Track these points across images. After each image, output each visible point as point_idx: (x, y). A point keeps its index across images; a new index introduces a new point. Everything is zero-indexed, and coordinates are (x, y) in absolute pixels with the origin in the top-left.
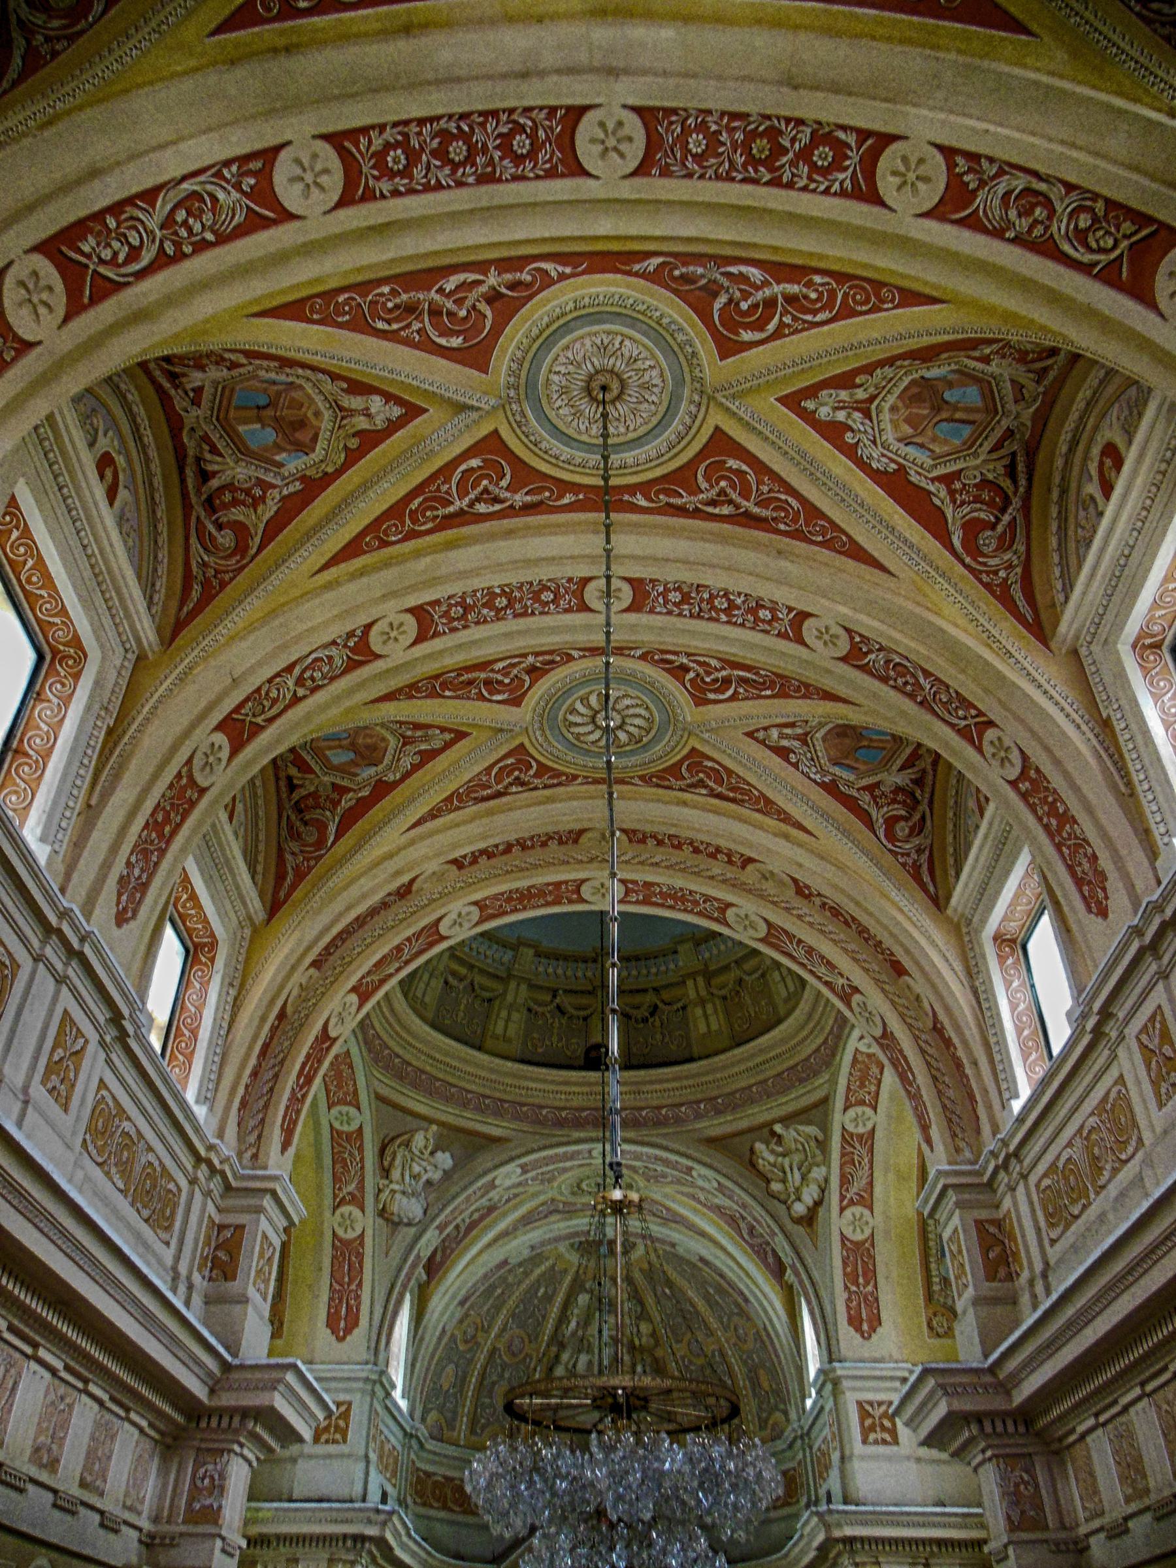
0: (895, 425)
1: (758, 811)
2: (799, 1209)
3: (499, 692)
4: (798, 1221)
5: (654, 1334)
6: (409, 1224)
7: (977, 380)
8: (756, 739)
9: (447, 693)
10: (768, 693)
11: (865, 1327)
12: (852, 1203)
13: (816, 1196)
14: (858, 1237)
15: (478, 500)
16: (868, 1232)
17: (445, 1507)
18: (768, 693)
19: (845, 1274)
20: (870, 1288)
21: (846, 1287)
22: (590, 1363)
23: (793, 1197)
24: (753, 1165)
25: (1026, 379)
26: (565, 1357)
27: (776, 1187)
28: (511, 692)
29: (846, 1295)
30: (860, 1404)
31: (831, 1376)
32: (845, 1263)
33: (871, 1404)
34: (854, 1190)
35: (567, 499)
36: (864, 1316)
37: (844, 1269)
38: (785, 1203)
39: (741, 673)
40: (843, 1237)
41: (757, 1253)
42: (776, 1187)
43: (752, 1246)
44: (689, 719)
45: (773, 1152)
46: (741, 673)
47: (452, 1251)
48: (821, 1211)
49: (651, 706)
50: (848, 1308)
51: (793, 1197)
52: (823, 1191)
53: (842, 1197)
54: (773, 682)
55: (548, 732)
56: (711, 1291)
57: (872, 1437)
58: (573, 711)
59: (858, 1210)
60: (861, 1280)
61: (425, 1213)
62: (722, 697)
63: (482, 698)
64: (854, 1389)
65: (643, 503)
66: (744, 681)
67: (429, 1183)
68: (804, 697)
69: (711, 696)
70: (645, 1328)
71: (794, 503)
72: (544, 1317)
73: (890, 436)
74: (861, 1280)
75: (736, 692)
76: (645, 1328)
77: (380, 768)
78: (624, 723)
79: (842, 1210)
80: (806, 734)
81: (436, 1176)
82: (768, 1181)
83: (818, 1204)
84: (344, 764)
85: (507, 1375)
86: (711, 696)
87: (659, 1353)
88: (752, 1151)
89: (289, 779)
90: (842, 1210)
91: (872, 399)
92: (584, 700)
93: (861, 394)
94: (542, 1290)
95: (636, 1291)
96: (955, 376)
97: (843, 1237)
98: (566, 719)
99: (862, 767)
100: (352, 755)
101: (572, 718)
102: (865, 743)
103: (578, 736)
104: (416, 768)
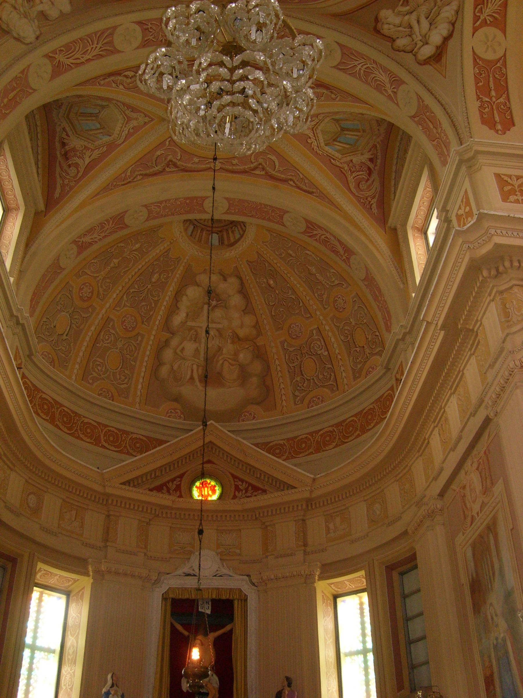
2: (427, 51)
4: (426, 62)
5: (257, 326)
6: (18, 39)
11: (499, 127)
12: (485, 23)
13: (445, 33)
14: (490, 56)
16: (500, 53)
17: (52, 421)
19: (477, 88)
20: (501, 100)
21: (478, 98)
22: (197, 350)
23: (420, 44)
24: (377, 31)
26: (174, 342)
27: (401, 42)
29: (478, 104)
30: (498, 176)
31: (466, 157)
32: (477, 80)
33: (510, 177)
34: (487, 11)
36: (497, 119)
37: (477, 84)
38: (411, 52)
40: (476, 57)
41: (363, 205)
42: (401, 42)
43: (358, 199)
45: (399, 14)
47: (71, 188)
48: (451, 43)
50: (482, 114)
51: (420, 44)
52: (453, 25)
53: (476, 18)
56: (313, 270)
57: (512, 198)
59: (491, 31)
60: (493, 93)
61: (37, 38)
64: (490, 165)
67: (43, 15)
70: (249, 320)
72: (156, 302)
74: (493, 93)
76: (249, 320)
79: (475, 30)
81: (53, 13)
82: (393, 40)
83: (446, 39)
85: (120, 345)
87: (260, 342)
88: (377, 20)
90: (475, 30)
94: (156, 276)
95: (242, 283)
97: (476, 57)
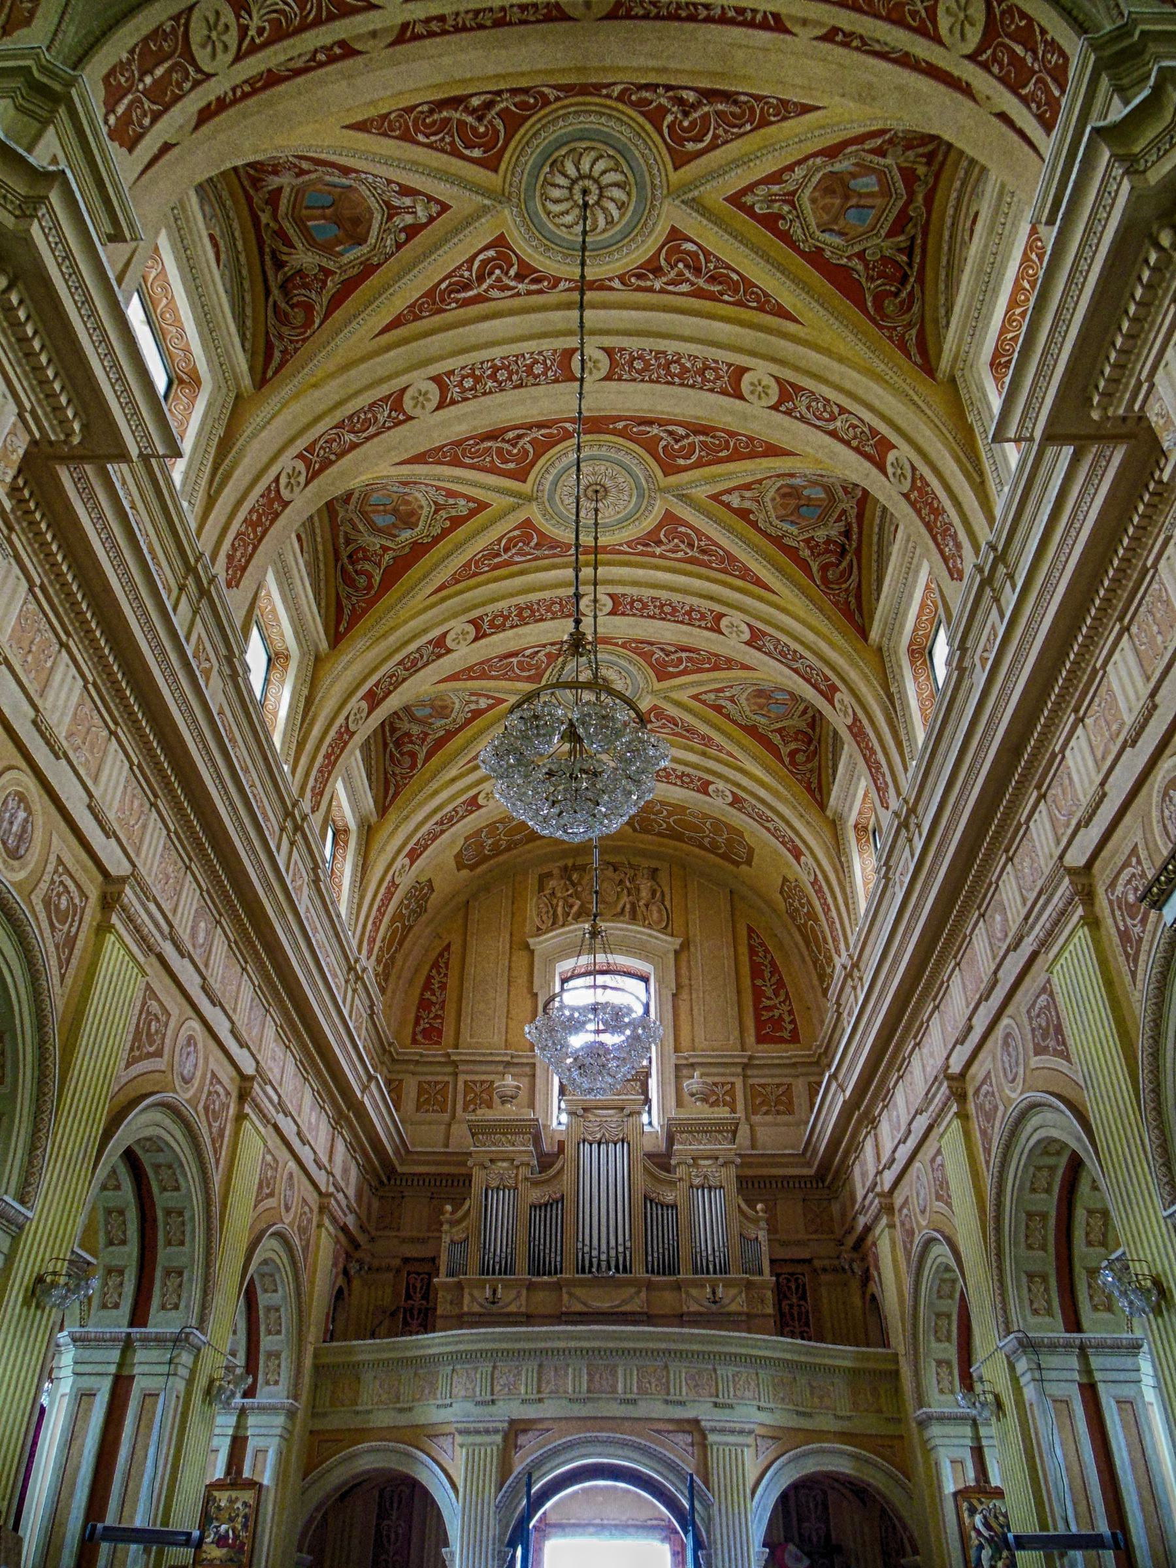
0: (416, 499)
1: (409, 110)
3: (688, 253)
7: (380, 530)
8: (438, 202)
9: (735, 277)
10: (443, 286)
15: (683, 437)
18: (443, 286)
25: (353, 535)
28: (676, 250)
35: (620, 425)
39: (471, 293)
44: (506, 212)
46: (471, 293)
49: (543, 216)
54: (442, 301)
55: (648, 179)
58: (621, 206)
62: (481, 257)
63: (707, 254)
65: (567, 425)
66: (466, 287)
68: (412, 306)
69: (491, 253)
71: (468, 461)
73: (419, 495)
75: (470, 269)
77: (829, 169)
78: (570, 189)
80: (390, 218)
84: (866, 175)
86: (491, 253)
89: (929, 164)
91: (436, 512)
92: (610, 222)
93: (443, 513)
96: (395, 532)
98: (629, 194)
99: (320, 186)
100: (852, 184)
101: (624, 197)
102: (328, 212)
103: (617, 169)
104: (790, 168)
